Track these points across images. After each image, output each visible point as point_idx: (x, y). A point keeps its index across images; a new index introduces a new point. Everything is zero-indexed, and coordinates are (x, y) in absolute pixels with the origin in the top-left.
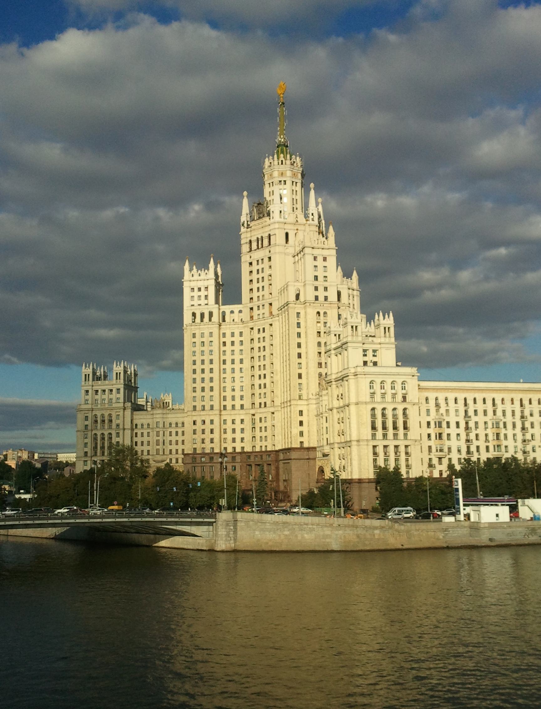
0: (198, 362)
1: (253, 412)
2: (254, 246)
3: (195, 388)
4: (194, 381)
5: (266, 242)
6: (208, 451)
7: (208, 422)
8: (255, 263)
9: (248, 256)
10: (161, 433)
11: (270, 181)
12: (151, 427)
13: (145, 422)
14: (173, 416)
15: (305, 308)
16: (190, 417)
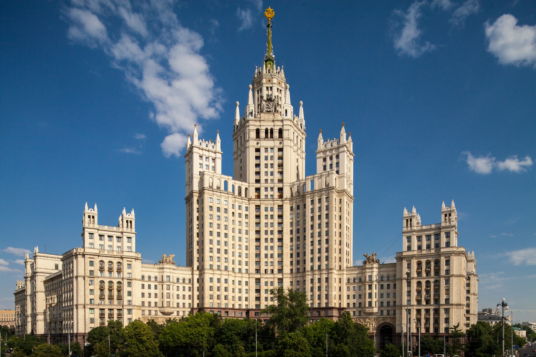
0: (215, 226)
1: (258, 276)
2: (262, 135)
3: (212, 248)
4: (211, 242)
5: (276, 135)
6: (223, 306)
7: (223, 281)
8: (262, 150)
9: (255, 142)
10: (171, 286)
12: (158, 280)
13: (153, 275)
14: (180, 272)
15: (339, 196)
16: (208, 274)
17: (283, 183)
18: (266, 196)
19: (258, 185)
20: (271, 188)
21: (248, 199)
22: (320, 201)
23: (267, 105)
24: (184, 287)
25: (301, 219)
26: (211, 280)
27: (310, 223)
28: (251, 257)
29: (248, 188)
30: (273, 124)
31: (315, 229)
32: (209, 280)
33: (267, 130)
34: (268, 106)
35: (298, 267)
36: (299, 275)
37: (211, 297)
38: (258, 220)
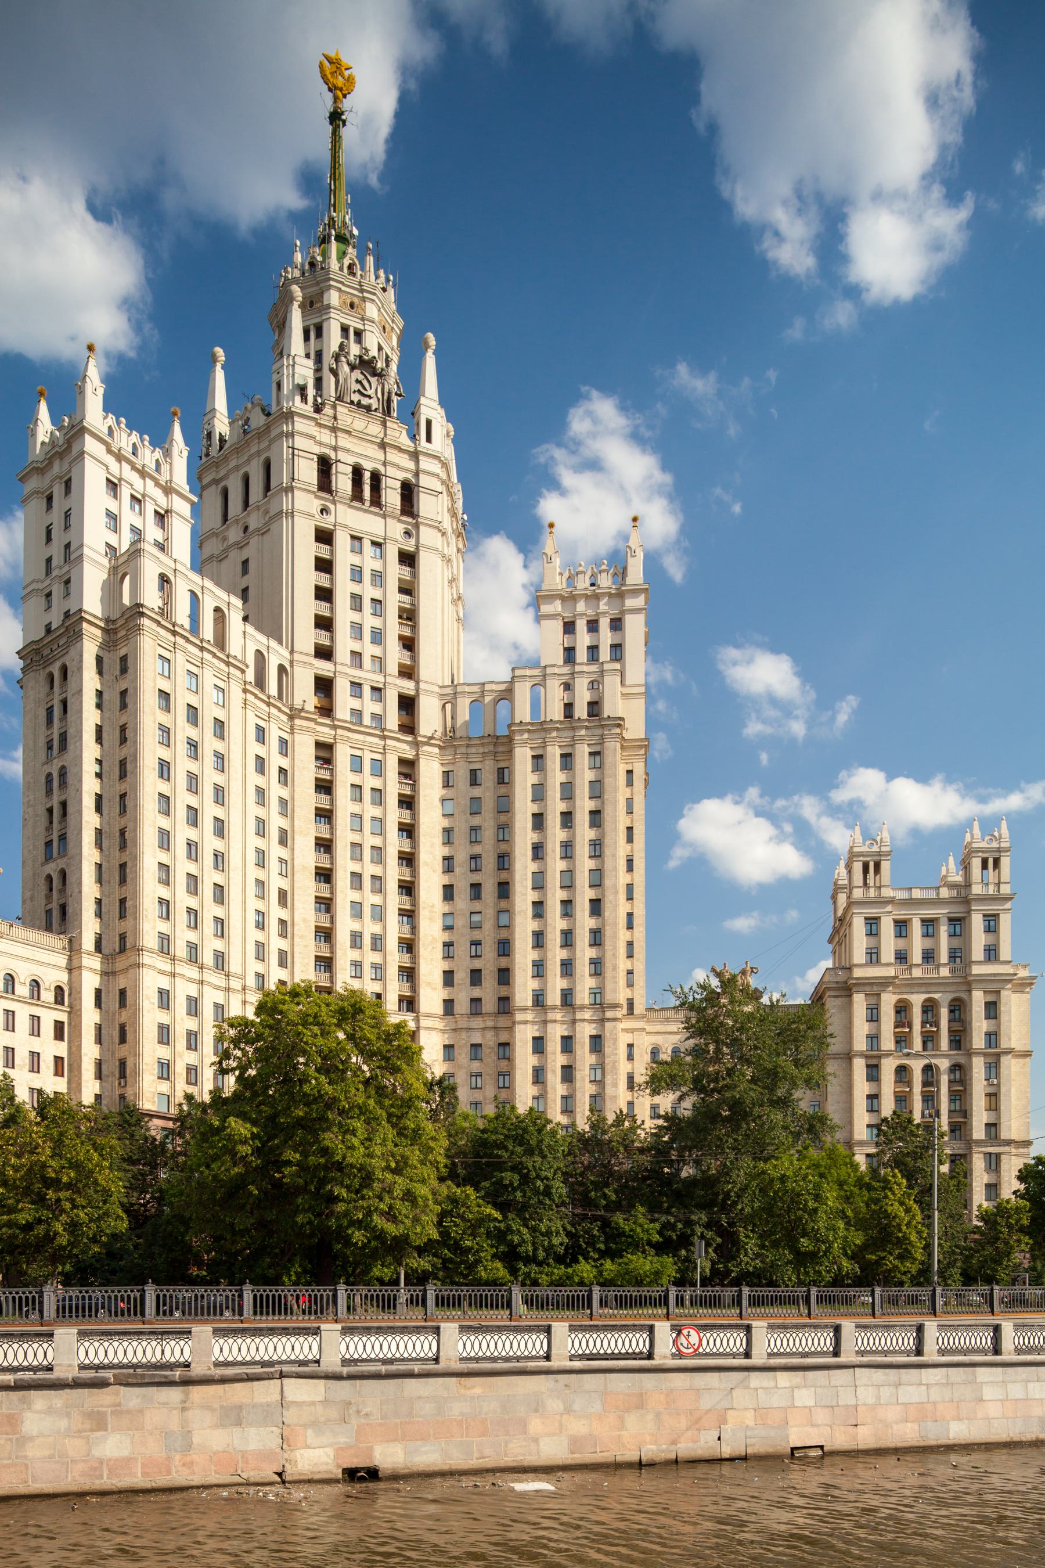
5: (392, 498)
8: (342, 540)
9: (316, 505)
11: (354, 323)
17: (418, 683)
18: (357, 714)
19: (324, 668)
20: (373, 688)
21: (288, 711)
22: (567, 758)
23: (358, 381)
24: (35, 1020)
25: (487, 821)
26: (165, 998)
27: (529, 837)
28: (302, 937)
29: (288, 668)
30: (380, 455)
31: (549, 859)
32: (155, 998)
33: (357, 472)
34: (358, 387)
35: (477, 993)
36: (477, 1022)
37: (165, 1070)
38: (324, 801)
